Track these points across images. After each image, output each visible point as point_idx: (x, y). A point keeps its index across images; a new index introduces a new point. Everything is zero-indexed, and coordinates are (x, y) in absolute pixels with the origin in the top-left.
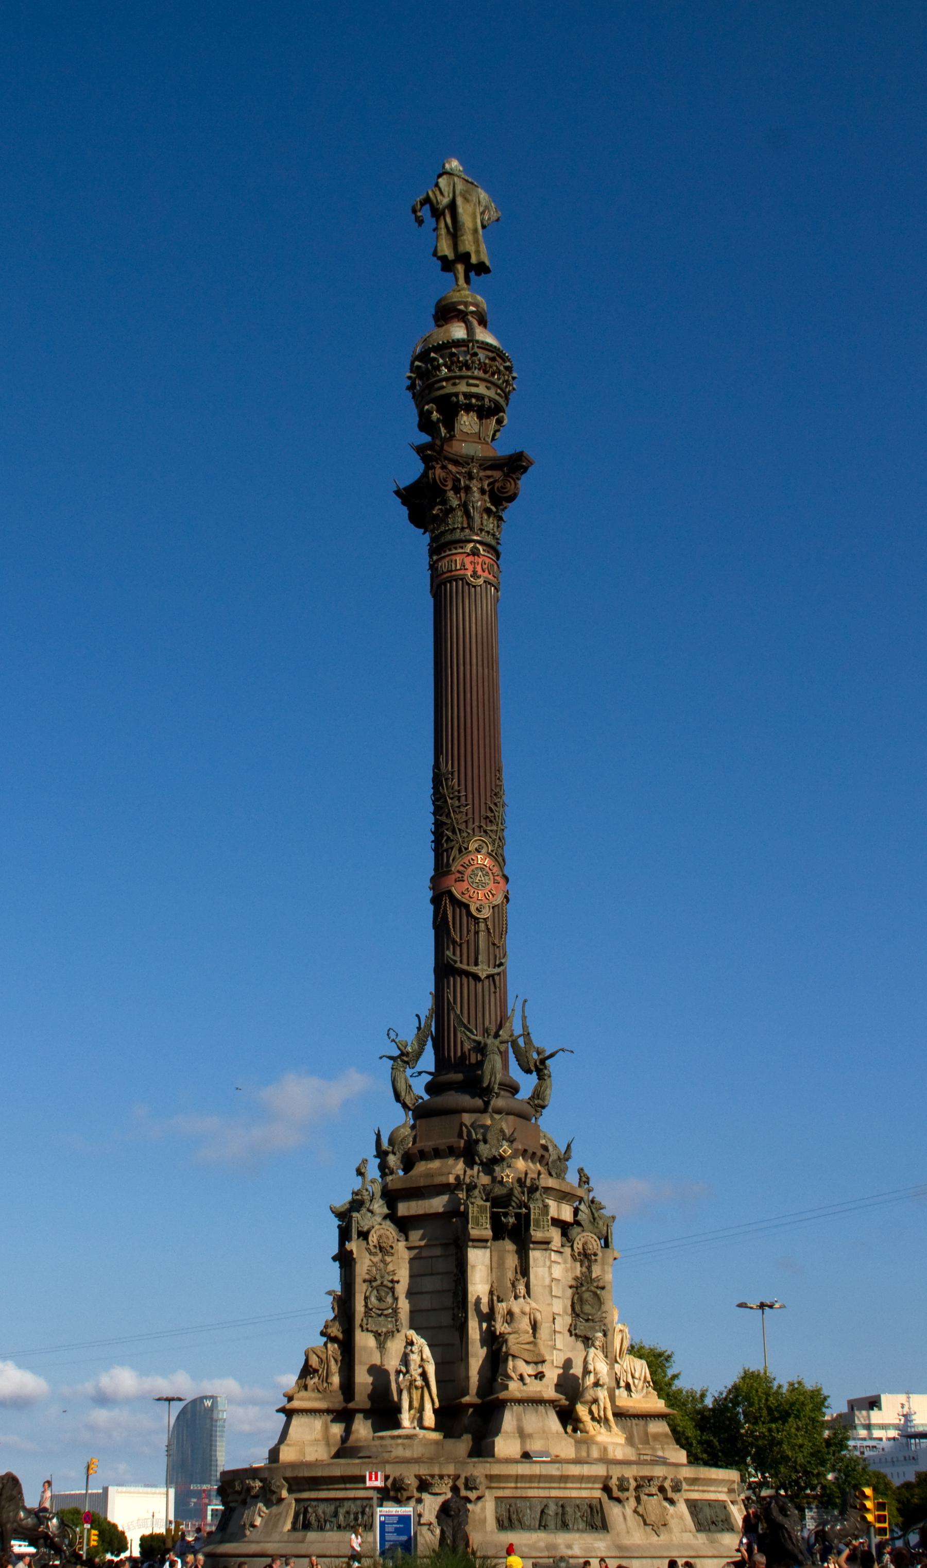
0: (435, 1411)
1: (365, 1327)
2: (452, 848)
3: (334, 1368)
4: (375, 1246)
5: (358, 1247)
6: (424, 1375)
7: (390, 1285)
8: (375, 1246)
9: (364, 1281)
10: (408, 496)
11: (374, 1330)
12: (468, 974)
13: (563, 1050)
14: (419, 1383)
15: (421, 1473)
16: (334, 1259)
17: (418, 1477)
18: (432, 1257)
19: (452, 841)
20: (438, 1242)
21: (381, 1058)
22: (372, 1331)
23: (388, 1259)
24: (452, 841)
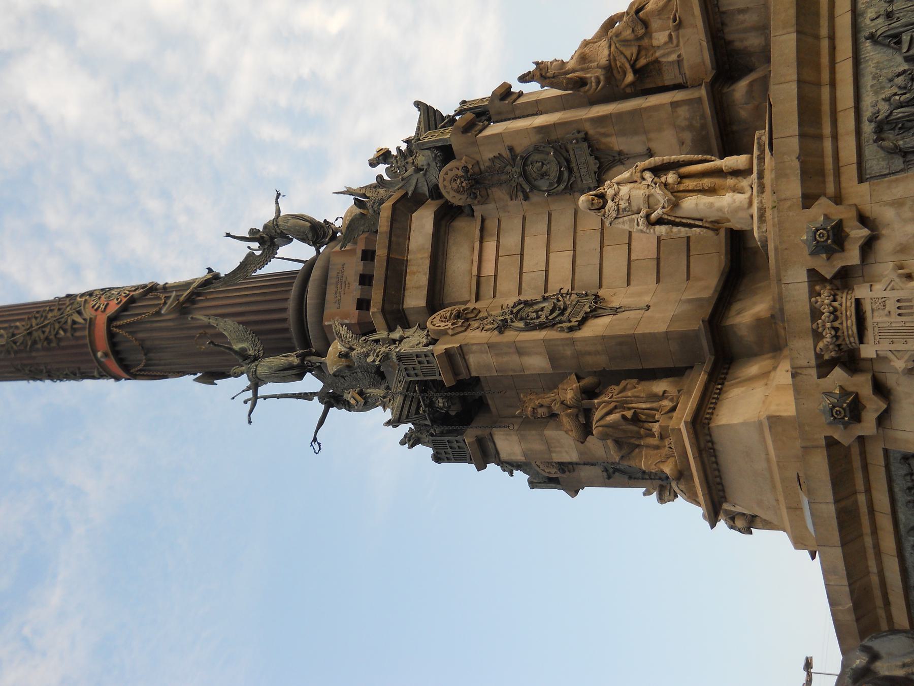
1: (573, 324)
6: (657, 171)
11: (582, 314)
14: (671, 177)
20: (477, 244)
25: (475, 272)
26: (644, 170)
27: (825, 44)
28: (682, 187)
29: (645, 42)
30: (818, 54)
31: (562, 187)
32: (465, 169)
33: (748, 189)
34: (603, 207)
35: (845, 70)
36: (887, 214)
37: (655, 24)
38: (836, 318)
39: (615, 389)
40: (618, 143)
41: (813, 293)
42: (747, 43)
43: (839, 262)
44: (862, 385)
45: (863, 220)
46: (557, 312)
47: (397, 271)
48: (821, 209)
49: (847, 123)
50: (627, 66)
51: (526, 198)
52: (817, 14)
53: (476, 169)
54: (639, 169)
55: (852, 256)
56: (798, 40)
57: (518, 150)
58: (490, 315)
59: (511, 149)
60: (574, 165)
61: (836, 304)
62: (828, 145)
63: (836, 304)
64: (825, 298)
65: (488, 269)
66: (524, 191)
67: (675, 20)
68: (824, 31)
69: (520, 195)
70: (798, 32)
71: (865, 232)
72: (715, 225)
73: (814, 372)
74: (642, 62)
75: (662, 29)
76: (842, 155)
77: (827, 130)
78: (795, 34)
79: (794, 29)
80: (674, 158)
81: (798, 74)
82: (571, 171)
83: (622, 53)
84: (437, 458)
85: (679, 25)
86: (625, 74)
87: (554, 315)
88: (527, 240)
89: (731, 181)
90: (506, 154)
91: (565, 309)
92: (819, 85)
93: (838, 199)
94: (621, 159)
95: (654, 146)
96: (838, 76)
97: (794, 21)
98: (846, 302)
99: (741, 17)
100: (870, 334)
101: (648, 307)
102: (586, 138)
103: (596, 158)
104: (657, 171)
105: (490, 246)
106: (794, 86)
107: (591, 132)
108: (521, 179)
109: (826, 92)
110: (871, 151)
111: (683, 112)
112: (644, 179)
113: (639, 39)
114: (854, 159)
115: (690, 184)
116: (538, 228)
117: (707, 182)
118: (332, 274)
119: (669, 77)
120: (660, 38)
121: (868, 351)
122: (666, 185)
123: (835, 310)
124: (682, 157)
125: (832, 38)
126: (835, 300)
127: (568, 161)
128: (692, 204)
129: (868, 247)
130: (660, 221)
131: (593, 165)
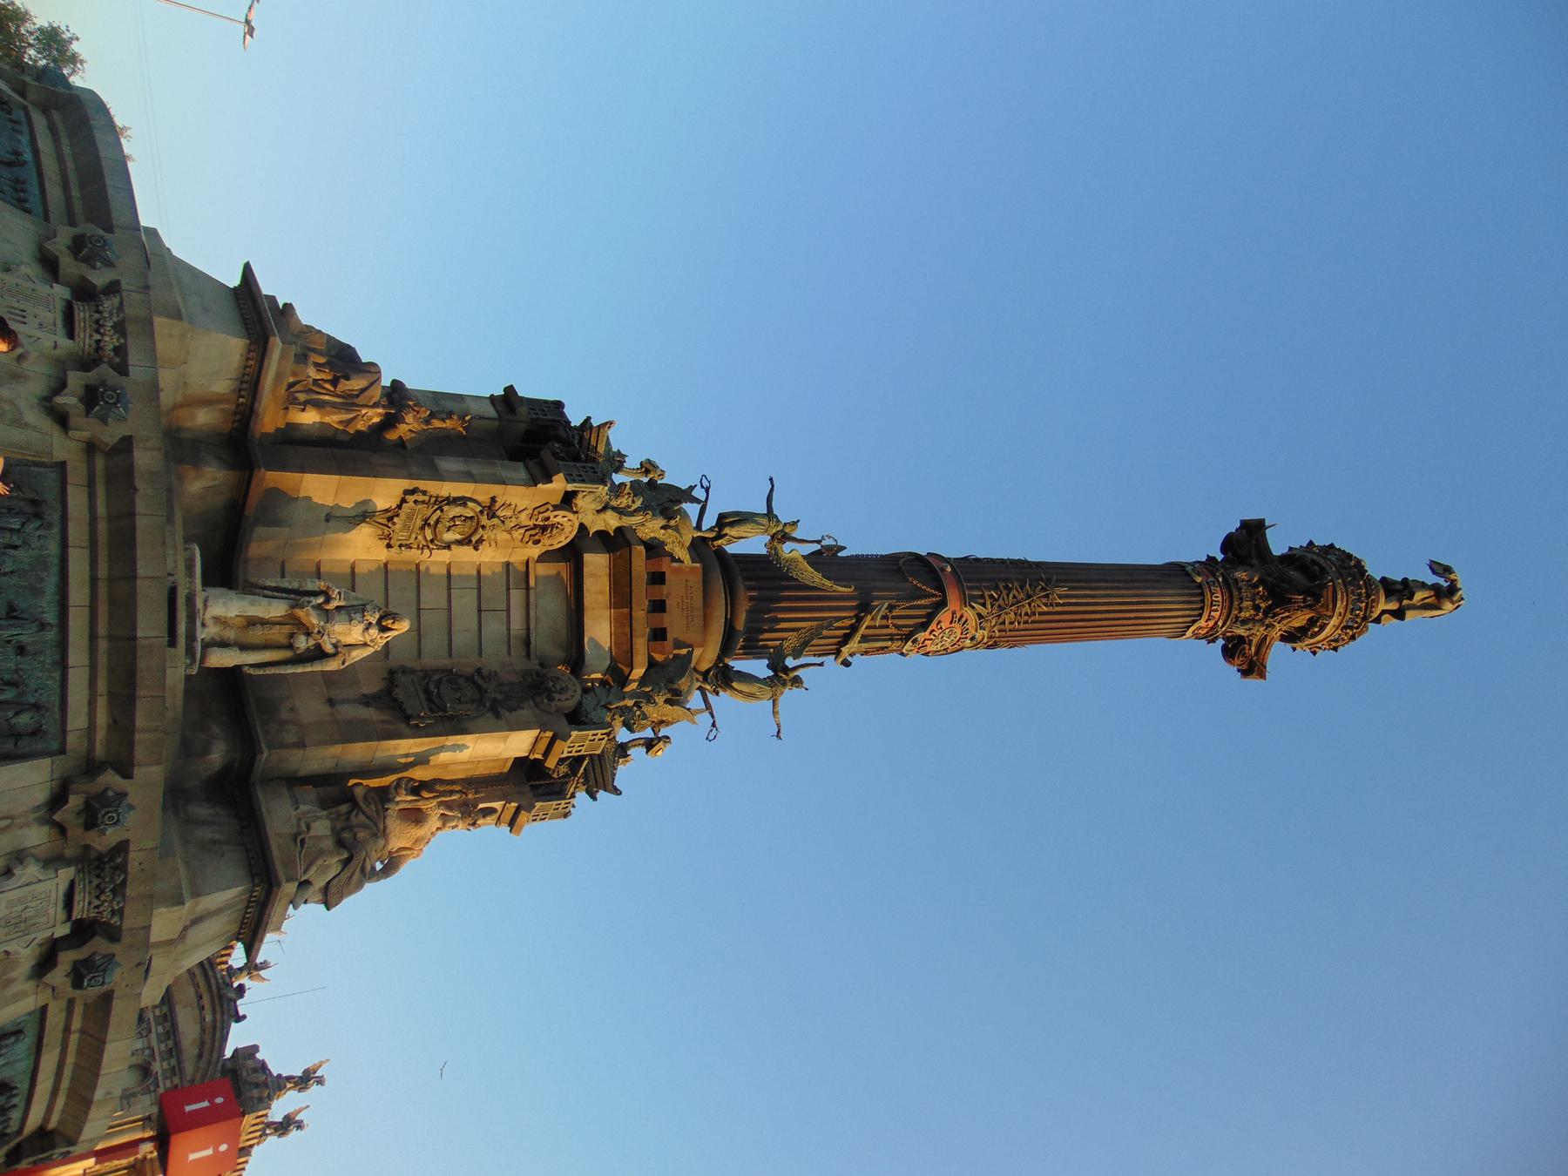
0: (237, 668)
1: (411, 498)
2: (984, 605)
3: (334, 419)
4: (548, 519)
5: (554, 490)
6: (318, 654)
7: (474, 539)
8: (548, 519)
9: (493, 499)
12: (854, 629)
13: (714, 725)
14: (302, 643)
15: (132, 855)
16: (510, 390)
17: (122, 848)
18: (508, 610)
22: (399, 507)
23: (518, 534)
25: (532, 592)
26: (334, 655)
27: (102, 630)
28: (287, 629)
29: (339, 826)
30: (111, 616)
31: (436, 677)
32: (551, 699)
33: (209, 622)
34: (381, 618)
35: (78, 595)
36: (33, 416)
37: (328, 844)
38: (97, 322)
39: (361, 426)
40: (370, 713)
41: (120, 350)
42: (212, 811)
43: (92, 376)
45: (62, 420)
46: (432, 522)
47: (621, 595)
48: (111, 434)
49: (77, 532)
50: (363, 805)
51: (479, 671)
52: (111, 671)
53: (538, 700)
54: (339, 659)
55: (76, 380)
56: (134, 627)
57: (489, 715)
58: (509, 532)
59: (498, 716)
60: (423, 697)
61: (97, 337)
62: (101, 509)
63: (97, 337)
64: (110, 341)
66: (482, 677)
67: (302, 842)
68: (103, 645)
69: (485, 673)
70: (134, 638)
71: (59, 400)
72: (251, 589)
73: (124, 285)
74: (344, 808)
75: (319, 838)
76: (84, 499)
77: (102, 527)
78: (140, 633)
79: (140, 642)
80: (300, 669)
81: (134, 587)
82: (427, 691)
83: (369, 818)
84: (559, 405)
85: (298, 839)
86: (365, 798)
87: (434, 518)
88: (475, 627)
89: (230, 635)
90: (503, 712)
91: (422, 528)
92: (111, 580)
94: (366, 701)
95: (326, 709)
96: (87, 590)
97: (139, 654)
98: (85, 340)
99: (217, 836)
100: (59, 305)
101: (327, 520)
102: (407, 718)
103: (395, 700)
104: (318, 654)
105: (517, 625)
106: (141, 571)
107: (402, 726)
108: (484, 686)
109: (103, 570)
110: (51, 496)
111: (290, 737)
112: (335, 646)
113: (343, 829)
114: (70, 489)
115: (278, 634)
116: (464, 637)
117: (257, 634)
118: (698, 622)
119: (310, 793)
120: (322, 828)
122: (308, 634)
123: (97, 331)
124: (290, 670)
125: (93, 637)
126: (98, 342)
127: (429, 700)
128: (276, 609)
130: (315, 594)
131: (399, 693)
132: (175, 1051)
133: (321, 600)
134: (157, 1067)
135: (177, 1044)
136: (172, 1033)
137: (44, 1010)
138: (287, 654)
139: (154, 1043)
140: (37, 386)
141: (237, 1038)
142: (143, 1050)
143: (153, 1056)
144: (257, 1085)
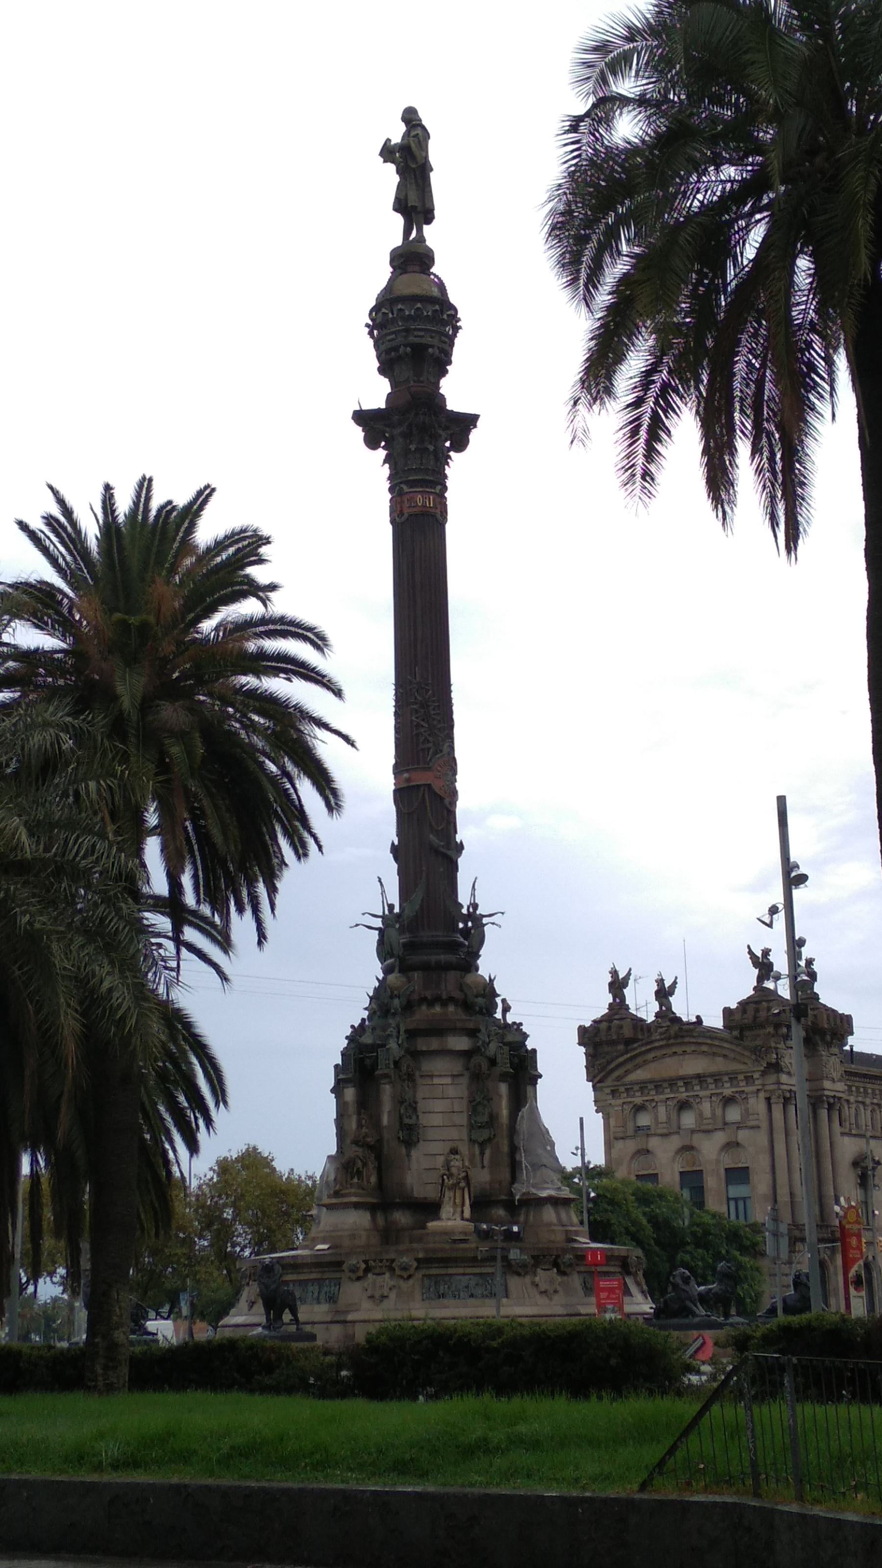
2: (429, 749)
10: (361, 417)
14: (463, 1184)
19: (428, 741)
21: (363, 914)
24: (428, 741)
36: (411, 1282)
41: (387, 1260)
44: (361, 1273)
64: (385, 1263)
65: (436, 1081)
82: (480, 1127)
89: (459, 1209)
93: (417, 1268)
98: (384, 1270)
100: (374, 1277)
105: (448, 1080)
121: (370, 1275)
122: (459, 1183)
124: (472, 1189)
129: (401, 1277)
131: (481, 1140)
132: (717, 1078)
133: (445, 1177)
134: (728, 1091)
135: (712, 1075)
136: (700, 1078)
137: (578, 1272)
138: (466, 1190)
139: (708, 1093)
140: (401, 1282)
141: (714, 1021)
142: (711, 1102)
143: (717, 1094)
144: (757, 1010)
